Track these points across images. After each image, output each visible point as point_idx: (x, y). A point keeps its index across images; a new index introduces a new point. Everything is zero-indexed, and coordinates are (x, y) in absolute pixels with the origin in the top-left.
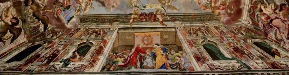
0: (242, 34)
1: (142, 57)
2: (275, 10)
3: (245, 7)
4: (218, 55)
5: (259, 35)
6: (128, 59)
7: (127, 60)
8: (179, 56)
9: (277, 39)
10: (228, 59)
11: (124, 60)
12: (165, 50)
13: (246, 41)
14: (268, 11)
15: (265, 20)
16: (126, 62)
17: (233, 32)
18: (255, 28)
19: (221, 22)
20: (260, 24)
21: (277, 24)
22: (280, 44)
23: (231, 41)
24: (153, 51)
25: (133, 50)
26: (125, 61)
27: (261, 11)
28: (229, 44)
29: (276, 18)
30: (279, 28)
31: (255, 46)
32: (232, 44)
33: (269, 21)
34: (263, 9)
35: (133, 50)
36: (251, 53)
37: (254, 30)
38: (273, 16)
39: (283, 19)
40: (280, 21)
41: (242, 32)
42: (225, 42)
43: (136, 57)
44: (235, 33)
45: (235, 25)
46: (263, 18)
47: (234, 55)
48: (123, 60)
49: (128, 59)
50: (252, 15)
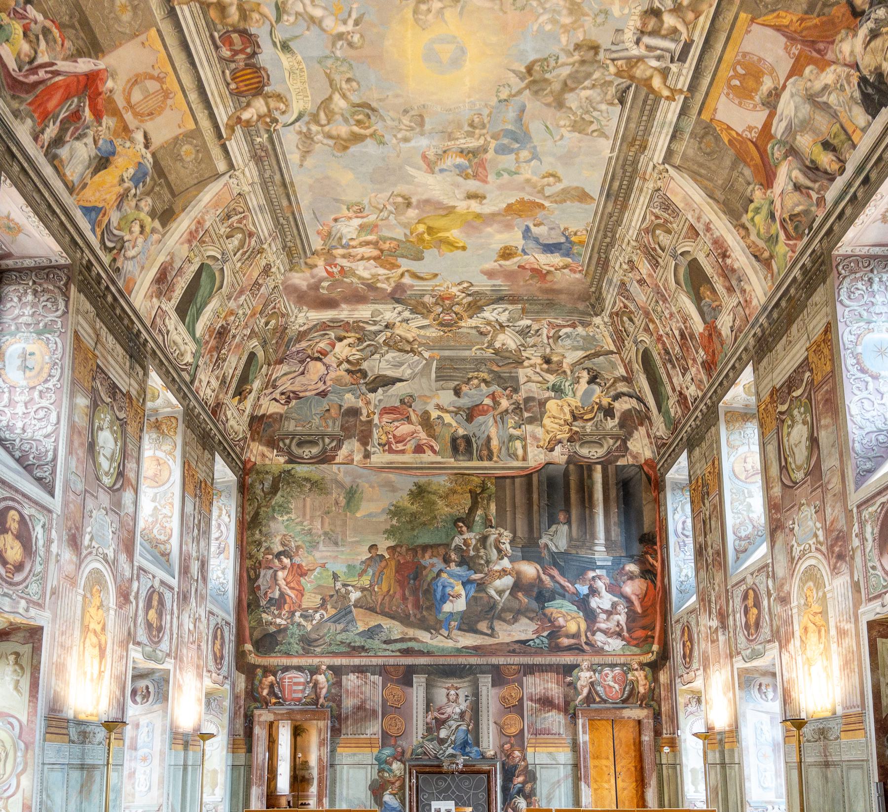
0: (267, 324)
1: (79, 118)
2: (348, 361)
3: (346, 313)
4: (192, 310)
5: (276, 351)
6: (42, 74)
7: (34, 71)
8: (142, 227)
9: (275, 380)
10: (192, 332)
11: (27, 59)
12: (138, 178)
13: (250, 337)
14: (342, 350)
15: (317, 348)
16: (26, 76)
17: (265, 305)
18: (290, 340)
19: (289, 275)
20: (304, 344)
21: (311, 370)
22: (266, 388)
23: (241, 312)
24: (118, 142)
25: (84, 65)
26: (27, 67)
27: (340, 339)
28: (231, 313)
29: (328, 367)
30: (303, 373)
31: (245, 358)
32: (232, 318)
33: (316, 355)
34: (346, 342)
35: (84, 65)
36: (224, 360)
37: (286, 339)
38: (330, 359)
39: (328, 378)
40: (321, 373)
41: (273, 322)
42: (232, 304)
43: (67, 97)
44: (267, 308)
45: (286, 304)
46: (322, 345)
47: (207, 337)
48: (26, 55)
49: (42, 74)
50: (324, 326)
